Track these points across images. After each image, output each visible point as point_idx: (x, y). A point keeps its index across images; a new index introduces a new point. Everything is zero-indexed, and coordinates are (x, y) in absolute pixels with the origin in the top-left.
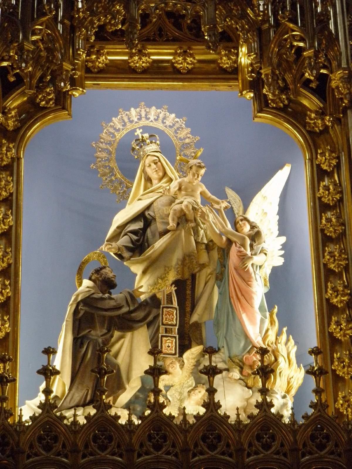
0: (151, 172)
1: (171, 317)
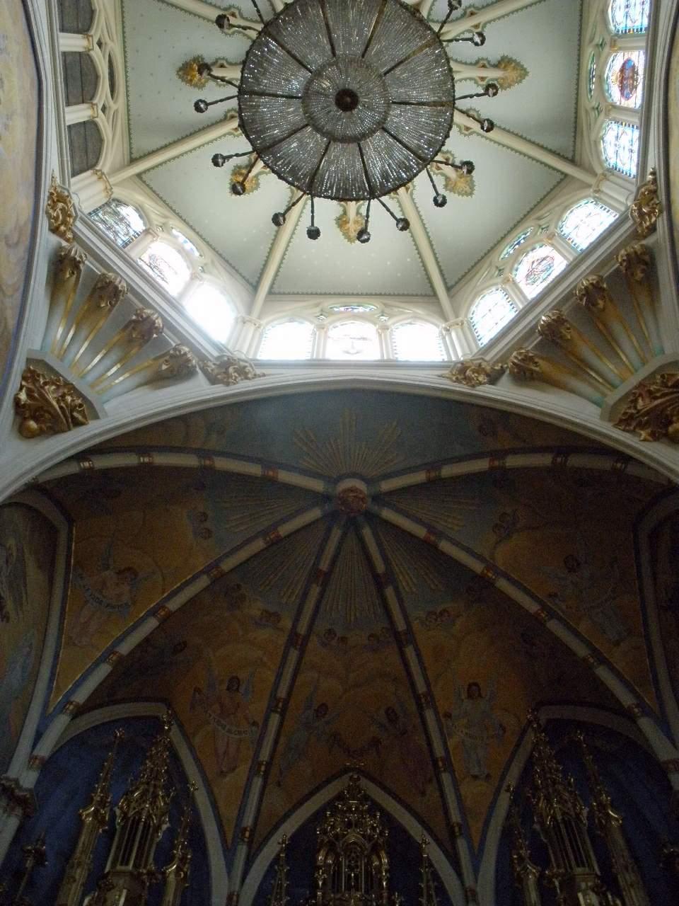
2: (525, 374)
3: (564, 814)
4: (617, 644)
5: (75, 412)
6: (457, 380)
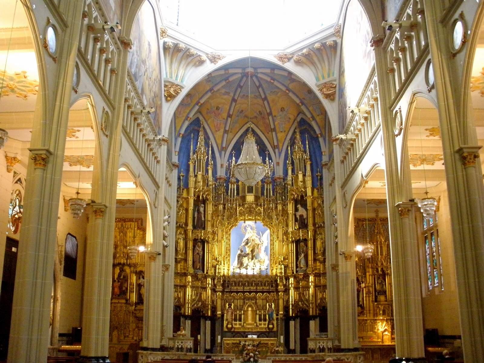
0: (249, 232)
1: (251, 256)
2: (298, 63)
3: (299, 157)
4: (318, 115)
6: (279, 60)
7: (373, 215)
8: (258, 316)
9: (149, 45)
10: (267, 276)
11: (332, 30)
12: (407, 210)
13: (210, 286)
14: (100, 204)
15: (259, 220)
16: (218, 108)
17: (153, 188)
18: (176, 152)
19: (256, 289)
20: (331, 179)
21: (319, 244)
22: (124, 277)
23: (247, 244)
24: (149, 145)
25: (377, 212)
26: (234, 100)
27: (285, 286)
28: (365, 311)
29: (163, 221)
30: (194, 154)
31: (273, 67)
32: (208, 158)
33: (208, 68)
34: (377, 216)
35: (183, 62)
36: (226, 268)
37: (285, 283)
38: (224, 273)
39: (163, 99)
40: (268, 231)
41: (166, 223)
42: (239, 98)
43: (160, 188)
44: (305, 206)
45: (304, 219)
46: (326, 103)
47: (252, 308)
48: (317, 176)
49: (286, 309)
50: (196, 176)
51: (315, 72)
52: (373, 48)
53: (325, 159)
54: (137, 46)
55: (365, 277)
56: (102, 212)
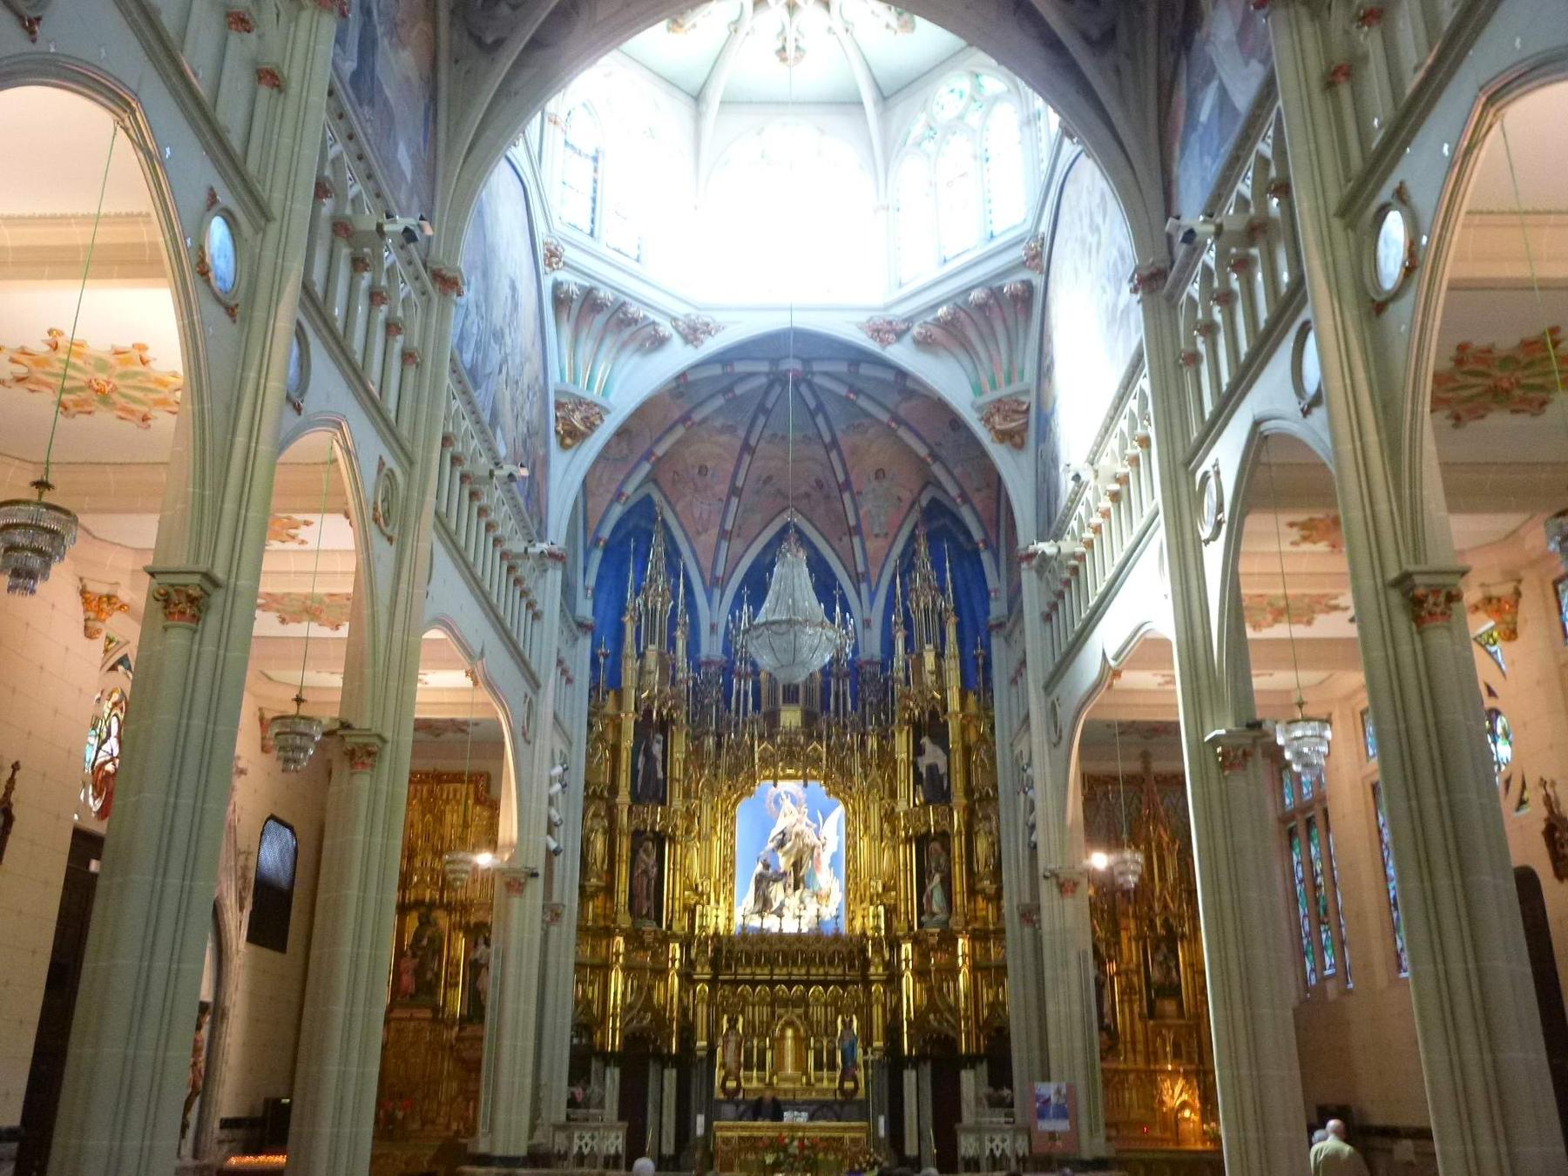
1: (791, 880)
2: (925, 343)
4: (978, 490)
5: (593, 414)
7: (1135, 767)
8: (811, 1055)
9: (513, 288)
10: (837, 937)
11: (1019, 253)
12: (1240, 753)
13: (677, 964)
14: (367, 733)
15: (814, 778)
16: (703, 470)
17: (523, 687)
18: (586, 589)
19: (808, 974)
20: (1014, 664)
21: (982, 846)
22: (431, 940)
23: (781, 844)
24: (511, 569)
25: (1146, 757)
26: (747, 448)
27: (888, 965)
28: (1121, 1046)
29: (546, 781)
30: (637, 595)
31: (857, 357)
32: (675, 607)
33: (677, 357)
34: (1147, 768)
35: (608, 342)
36: (723, 914)
37: (887, 956)
38: (716, 928)
39: (553, 440)
40: (841, 809)
41: (557, 787)
42: (762, 444)
43: (541, 691)
44: (941, 739)
45: (941, 778)
46: (999, 454)
47: (796, 1030)
48: (976, 658)
49: (892, 1032)
50: (641, 656)
51: (970, 368)
52: (1138, 297)
53: (997, 609)
54: (477, 291)
55: (1118, 943)
56: (370, 754)
